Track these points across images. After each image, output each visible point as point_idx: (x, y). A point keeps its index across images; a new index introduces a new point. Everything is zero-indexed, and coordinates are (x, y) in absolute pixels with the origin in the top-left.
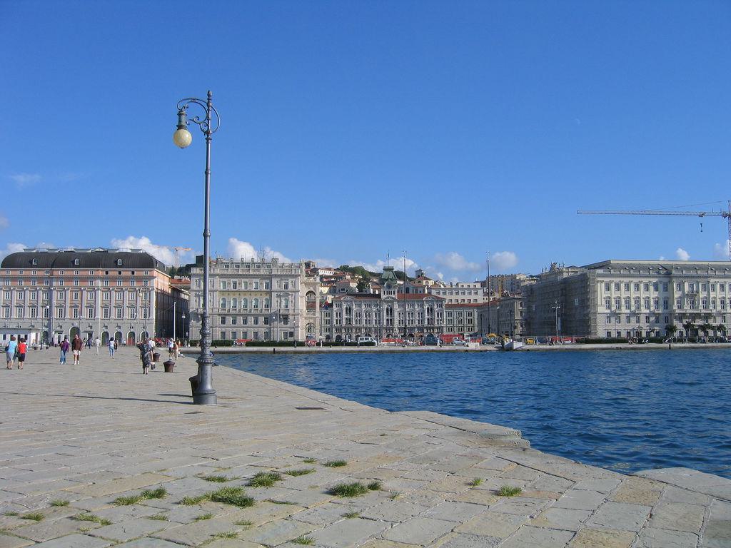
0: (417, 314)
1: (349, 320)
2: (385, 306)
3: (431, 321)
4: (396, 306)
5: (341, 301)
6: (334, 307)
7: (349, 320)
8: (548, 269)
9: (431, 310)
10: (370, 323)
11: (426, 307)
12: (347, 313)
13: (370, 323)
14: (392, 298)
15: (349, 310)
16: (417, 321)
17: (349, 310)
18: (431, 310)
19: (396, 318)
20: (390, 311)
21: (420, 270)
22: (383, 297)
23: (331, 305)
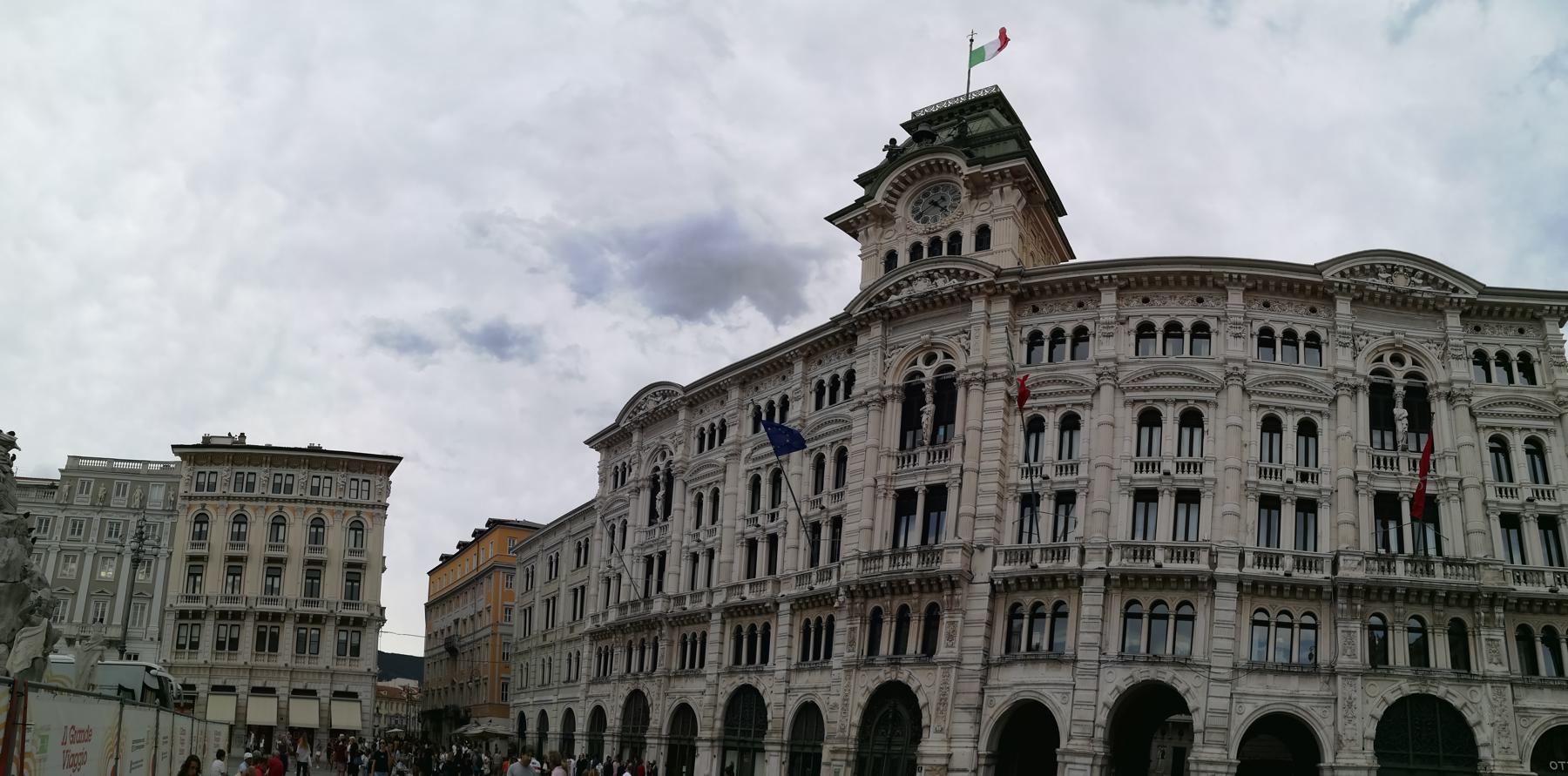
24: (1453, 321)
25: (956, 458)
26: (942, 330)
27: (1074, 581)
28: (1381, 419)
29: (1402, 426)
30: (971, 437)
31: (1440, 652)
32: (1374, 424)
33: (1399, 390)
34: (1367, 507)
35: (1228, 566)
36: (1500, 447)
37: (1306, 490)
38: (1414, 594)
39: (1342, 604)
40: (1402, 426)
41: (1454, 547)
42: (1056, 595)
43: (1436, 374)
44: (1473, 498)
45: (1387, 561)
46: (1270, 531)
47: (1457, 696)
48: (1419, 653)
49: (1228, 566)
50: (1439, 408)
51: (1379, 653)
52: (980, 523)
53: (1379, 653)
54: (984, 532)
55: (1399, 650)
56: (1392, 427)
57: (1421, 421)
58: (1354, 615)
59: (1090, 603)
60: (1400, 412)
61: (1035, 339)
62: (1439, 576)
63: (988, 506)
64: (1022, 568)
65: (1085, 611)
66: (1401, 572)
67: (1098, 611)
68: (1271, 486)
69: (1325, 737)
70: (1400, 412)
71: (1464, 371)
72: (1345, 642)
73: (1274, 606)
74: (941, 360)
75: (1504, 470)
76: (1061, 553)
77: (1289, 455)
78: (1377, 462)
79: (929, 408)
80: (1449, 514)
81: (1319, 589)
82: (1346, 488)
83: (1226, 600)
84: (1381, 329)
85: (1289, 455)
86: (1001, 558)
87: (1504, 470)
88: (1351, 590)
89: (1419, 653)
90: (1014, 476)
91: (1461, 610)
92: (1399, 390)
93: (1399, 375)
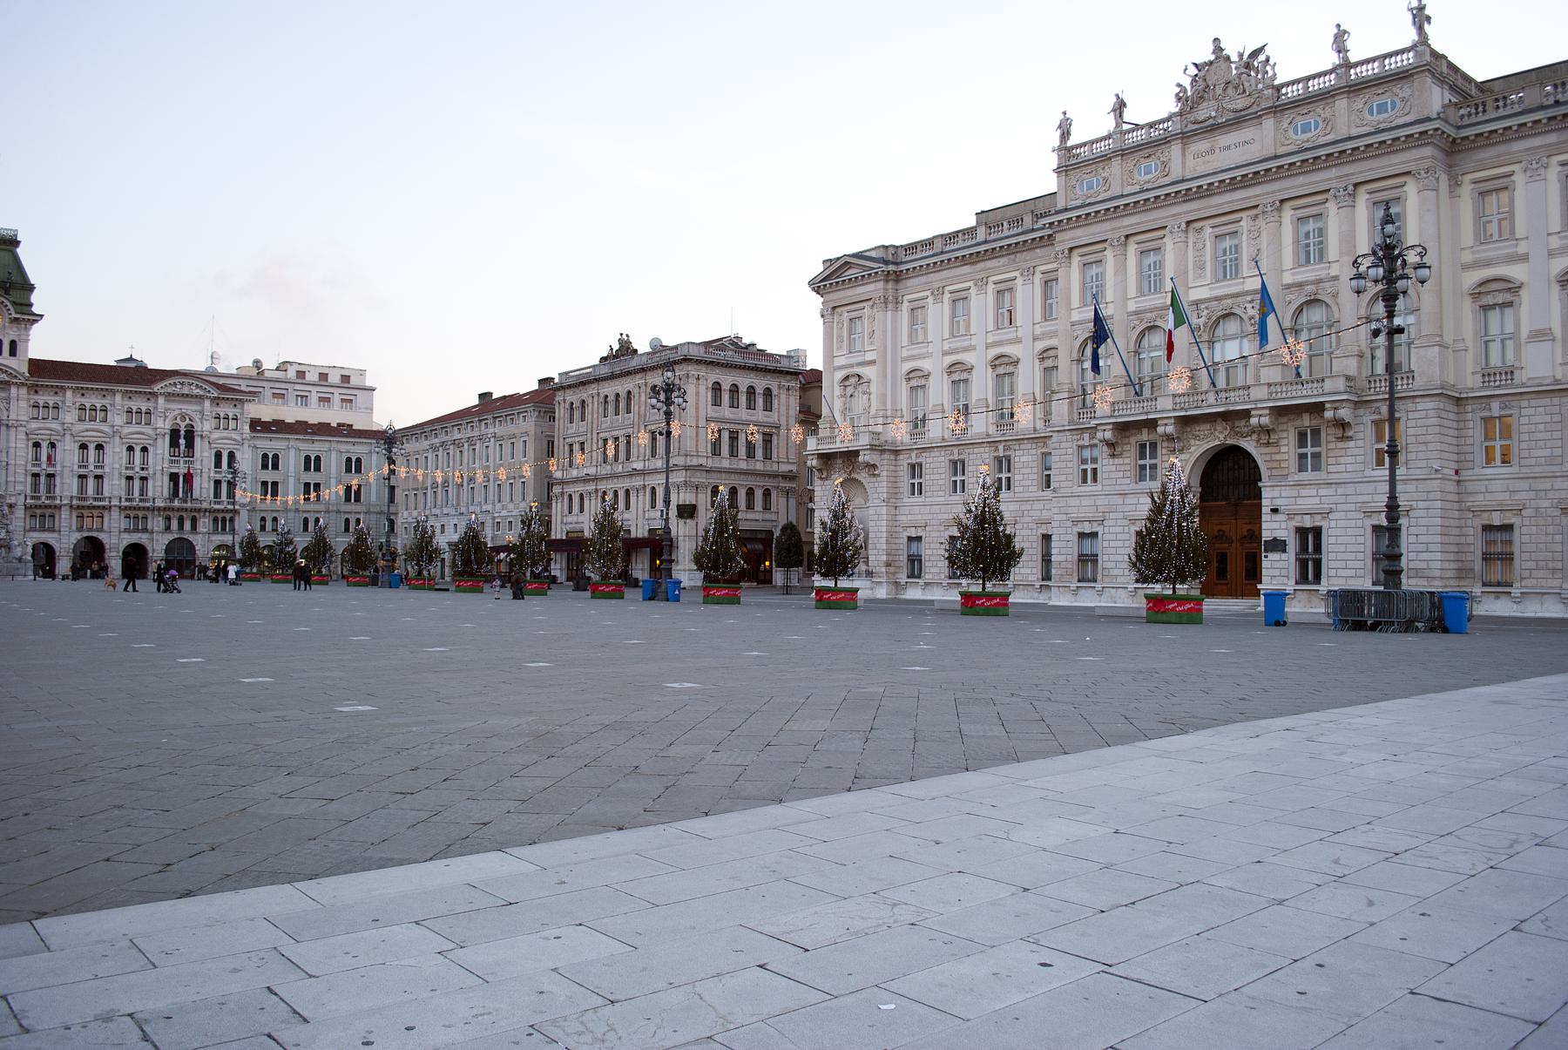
3: (181, 483)
8: (1154, 103)
9: (183, 439)
11: (164, 425)
27: (59, 507)
28: (174, 443)
29: (182, 447)
30: (12, 451)
31: (187, 525)
34: (166, 478)
35: (115, 502)
36: (218, 455)
37: (144, 473)
40: (182, 447)
41: (196, 494)
43: (198, 428)
44: (205, 476)
45: (172, 501)
48: (181, 526)
49: (115, 502)
50: (197, 441)
51: (168, 528)
53: (168, 528)
54: (19, 488)
55: (175, 524)
56: (178, 446)
57: (190, 444)
59: (65, 513)
60: (182, 441)
66: (176, 503)
68: (130, 473)
69: (149, 548)
70: (182, 441)
72: (157, 523)
75: (218, 464)
76: (54, 498)
77: (137, 462)
80: (196, 482)
82: (159, 474)
83: (115, 513)
84: (177, 407)
85: (137, 462)
87: (218, 464)
88: (159, 509)
89: (181, 526)
90: (29, 467)
93: (183, 425)
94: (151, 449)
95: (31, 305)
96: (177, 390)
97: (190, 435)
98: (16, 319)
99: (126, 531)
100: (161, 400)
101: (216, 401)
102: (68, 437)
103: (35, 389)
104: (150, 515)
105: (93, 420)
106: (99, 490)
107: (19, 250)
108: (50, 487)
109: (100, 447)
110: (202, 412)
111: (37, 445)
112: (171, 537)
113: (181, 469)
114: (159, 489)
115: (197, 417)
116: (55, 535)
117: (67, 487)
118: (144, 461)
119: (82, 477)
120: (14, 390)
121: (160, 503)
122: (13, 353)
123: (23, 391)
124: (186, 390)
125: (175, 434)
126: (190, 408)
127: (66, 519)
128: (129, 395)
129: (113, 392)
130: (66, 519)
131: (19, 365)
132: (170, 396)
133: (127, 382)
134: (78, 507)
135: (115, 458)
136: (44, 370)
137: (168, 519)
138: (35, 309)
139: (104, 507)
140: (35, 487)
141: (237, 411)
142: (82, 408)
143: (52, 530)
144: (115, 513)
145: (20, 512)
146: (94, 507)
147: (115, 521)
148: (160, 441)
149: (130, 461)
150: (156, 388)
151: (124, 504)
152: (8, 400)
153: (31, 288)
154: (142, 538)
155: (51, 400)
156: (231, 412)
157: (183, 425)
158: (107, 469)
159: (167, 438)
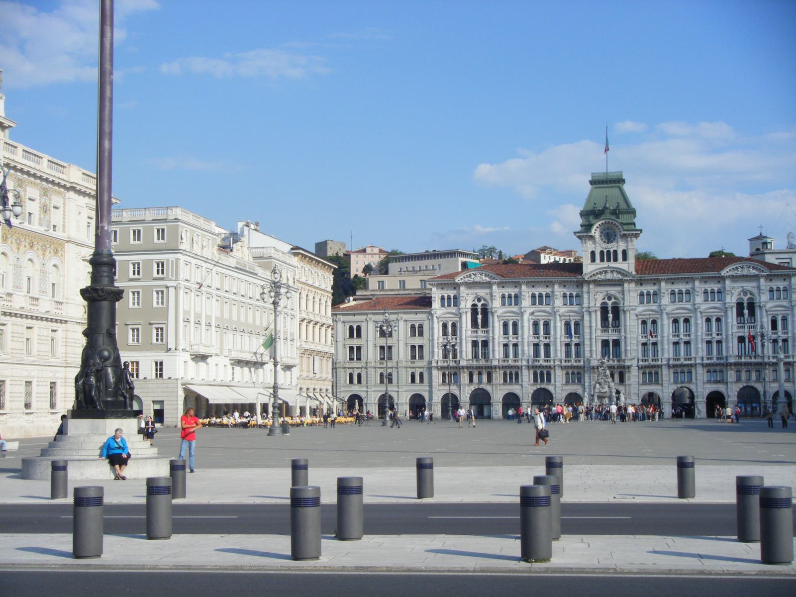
0: (701, 322)
1: (482, 347)
2: (595, 298)
4: (631, 296)
5: (456, 286)
6: (436, 304)
7: (482, 347)
9: (747, 309)
10: (547, 354)
11: (731, 300)
12: (474, 323)
13: (547, 354)
14: (619, 271)
15: (481, 316)
16: (702, 347)
17: (481, 316)
18: (747, 309)
19: (632, 333)
20: (612, 315)
21: (761, 237)
22: (589, 268)
23: (424, 302)
24: (762, 281)
25: (623, 331)
26: (613, 290)
27: (660, 367)
28: (740, 314)
29: (746, 316)
32: (738, 316)
33: (745, 305)
35: (699, 361)
38: (746, 364)
39: (729, 368)
40: (746, 316)
42: (655, 369)
45: (740, 357)
46: (709, 351)
47: (759, 387)
48: (749, 379)
51: (738, 380)
52: (632, 352)
54: (634, 354)
57: (752, 313)
58: (731, 369)
59: (665, 371)
60: (746, 311)
61: (642, 294)
62: (753, 360)
63: (635, 347)
64: (646, 363)
65: (664, 373)
66: (743, 360)
67: (667, 373)
70: (746, 311)
71: (764, 297)
72: (731, 375)
73: (712, 369)
74: (613, 300)
77: (714, 329)
78: (739, 327)
79: (610, 316)
81: (723, 364)
85: (714, 329)
86: (640, 361)
88: (731, 364)
90: (640, 339)
91: (760, 367)
92: (745, 305)
94: (723, 320)
95: (634, 224)
96: (739, 272)
97: (752, 307)
98: (625, 235)
99: (709, 382)
100: (728, 282)
101: (769, 278)
102: (665, 316)
103: (640, 282)
104: (724, 369)
105: (680, 301)
106: (688, 352)
107: (626, 188)
108: (655, 353)
109: (687, 321)
110: (759, 288)
111: (644, 322)
112: (741, 385)
113: (745, 333)
114: (732, 350)
115: (755, 291)
116: (660, 387)
117: (667, 353)
118: (719, 329)
119: (676, 344)
120: (626, 285)
121: (731, 360)
122: (625, 258)
123: (633, 285)
124: (745, 272)
125: (740, 305)
126: (749, 286)
127: (666, 375)
128: (704, 280)
129: (693, 280)
130: (666, 375)
131: (629, 266)
132: (734, 278)
133: (703, 270)
134: (674, 366)
135: (699, 328)
136: (651, 268)
137: (738, 371)
138: (638, 227)
139: (691, 365)
140: (645, 353)
141: (786, 283)
142: (673, 293)
143: (657, 382)
144: (700, 370)
145: (634, 371)
146: (684, 365)
147: (701, 374)
148: (729, 313)
149: (709, 329)
150: (723, 273)
151: (706, 361)
152: (623, 292)
153: (633, 212)
154: (721, 388)
155: (651, 288)
156: (781, 284)
157: (745, 298)
158: (692, 337)
159: (735, 310)
